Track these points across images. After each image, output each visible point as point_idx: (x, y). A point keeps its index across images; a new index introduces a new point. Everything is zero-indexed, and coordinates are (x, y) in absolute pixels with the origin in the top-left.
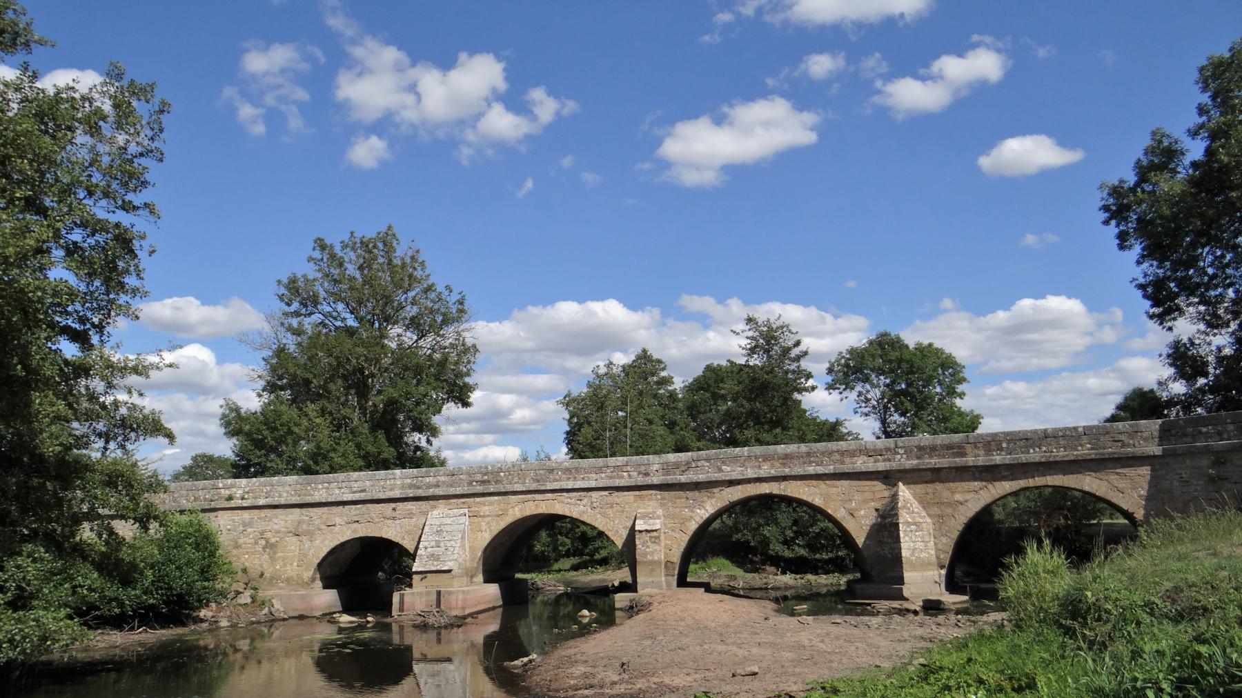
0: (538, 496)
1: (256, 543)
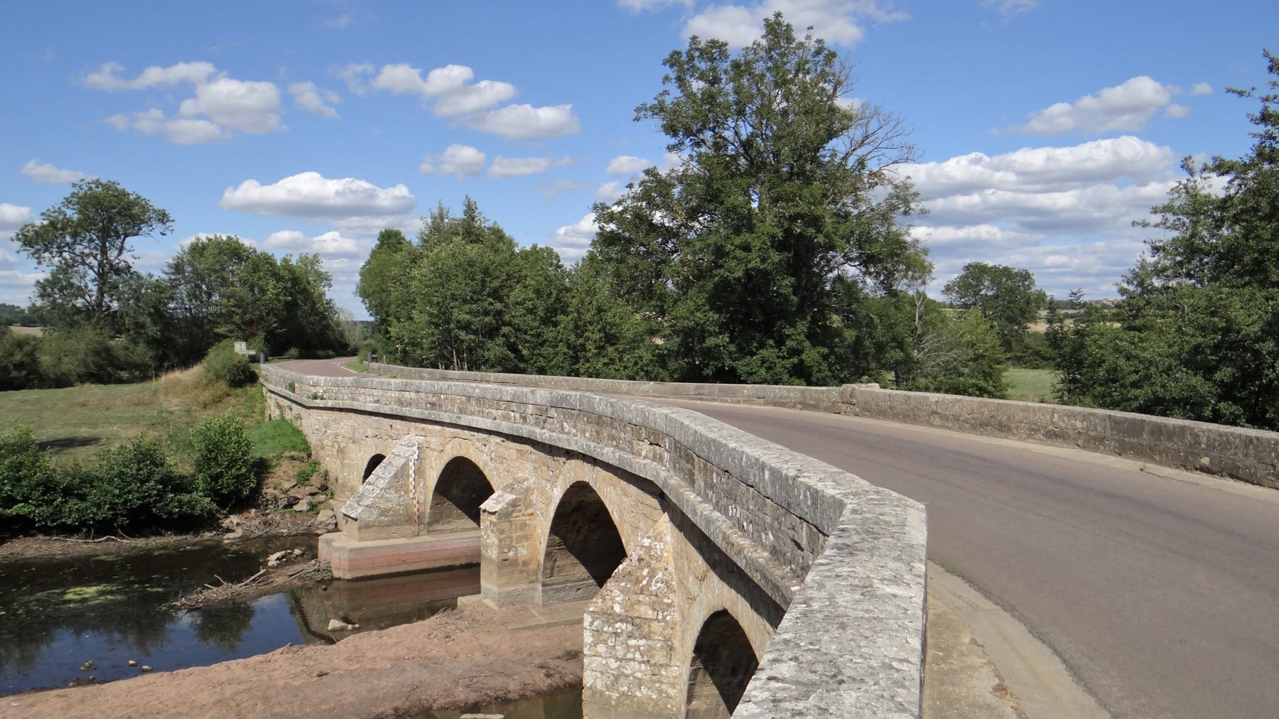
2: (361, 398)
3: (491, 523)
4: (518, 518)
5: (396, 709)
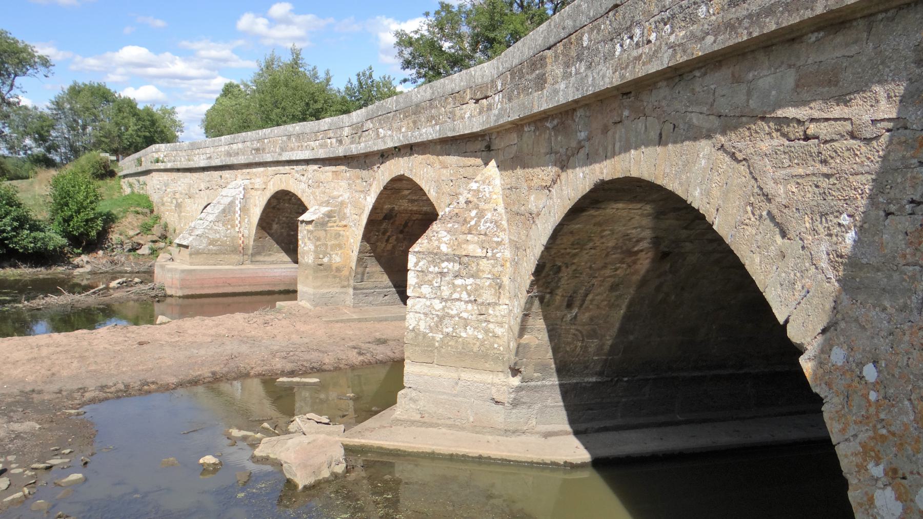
0: (281, 169)
1: (172, 202)
2: (195, 159)
3: (308, 231)
4: (333, 228)
5: (214, 373)
